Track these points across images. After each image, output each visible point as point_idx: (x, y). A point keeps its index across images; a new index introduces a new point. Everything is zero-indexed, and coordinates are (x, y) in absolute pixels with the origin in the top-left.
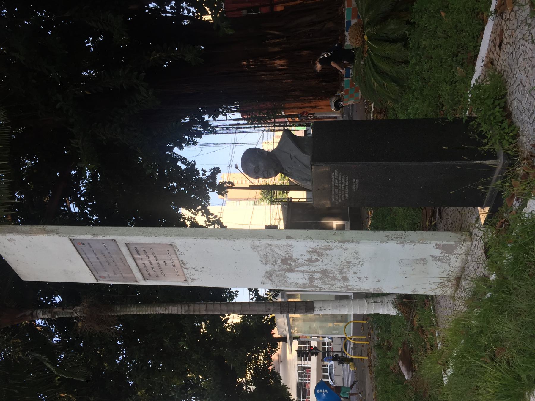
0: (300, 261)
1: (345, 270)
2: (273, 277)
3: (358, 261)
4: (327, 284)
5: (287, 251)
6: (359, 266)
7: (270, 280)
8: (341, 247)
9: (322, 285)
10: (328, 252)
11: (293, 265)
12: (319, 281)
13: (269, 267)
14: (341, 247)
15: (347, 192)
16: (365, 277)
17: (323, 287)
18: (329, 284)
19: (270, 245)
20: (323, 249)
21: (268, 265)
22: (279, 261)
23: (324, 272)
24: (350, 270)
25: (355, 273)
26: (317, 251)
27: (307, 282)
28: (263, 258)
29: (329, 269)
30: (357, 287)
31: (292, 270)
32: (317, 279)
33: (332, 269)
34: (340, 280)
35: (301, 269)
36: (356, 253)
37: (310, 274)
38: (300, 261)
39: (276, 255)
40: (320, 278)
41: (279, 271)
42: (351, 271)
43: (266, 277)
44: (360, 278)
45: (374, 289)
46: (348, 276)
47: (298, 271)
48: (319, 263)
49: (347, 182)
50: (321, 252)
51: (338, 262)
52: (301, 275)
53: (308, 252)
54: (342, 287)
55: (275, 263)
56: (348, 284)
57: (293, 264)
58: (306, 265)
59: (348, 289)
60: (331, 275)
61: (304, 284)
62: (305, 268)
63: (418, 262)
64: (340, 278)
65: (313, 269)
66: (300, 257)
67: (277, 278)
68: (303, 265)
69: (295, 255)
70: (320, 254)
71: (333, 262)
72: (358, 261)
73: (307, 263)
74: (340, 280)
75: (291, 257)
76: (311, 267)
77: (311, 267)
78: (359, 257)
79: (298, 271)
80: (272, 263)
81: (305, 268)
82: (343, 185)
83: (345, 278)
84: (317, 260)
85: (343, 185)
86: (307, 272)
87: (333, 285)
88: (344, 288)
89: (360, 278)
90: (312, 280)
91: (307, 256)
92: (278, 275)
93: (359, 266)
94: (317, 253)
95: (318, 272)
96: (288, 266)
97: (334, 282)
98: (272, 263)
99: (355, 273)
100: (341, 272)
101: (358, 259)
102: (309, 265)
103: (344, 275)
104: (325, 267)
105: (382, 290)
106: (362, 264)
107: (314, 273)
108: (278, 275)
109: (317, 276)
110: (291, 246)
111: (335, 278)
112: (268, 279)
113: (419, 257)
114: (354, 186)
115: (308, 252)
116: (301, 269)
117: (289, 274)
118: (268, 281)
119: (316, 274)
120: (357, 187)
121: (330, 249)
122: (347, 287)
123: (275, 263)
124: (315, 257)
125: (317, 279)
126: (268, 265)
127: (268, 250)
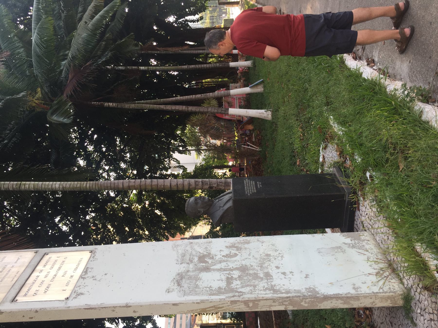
0: (218, 257)
1: (266, 265)
2: (184, 280)
3: (277, 253)
4: (247, 286)
5: (206, 248)
6: (280, 258)
7: (179, 285)
8: (258, 240)
9: (242, 287)
10: (246, 246)
11: (210, 262)
12: (238, 282)
13: (182, 268)
14: (258, 240)
15: (255, 188)
16: (291, 272)
17: (243, 290)
18: (251, 286)
19: (192, 243)
20: (242, 243)
21: (183, 264)
22: (196, 259)
23: (243, 269)
24: (272, 264)
25: (277, 267)
26: (236, 245)
27: (223, 284)
28: (180, 257)
29: (248, 264)
30: (285, 287)
31: (207, 269)
32: (236, 279)
33: (252, 264)
34: (262, 279)
35: (218, 266)
36: (273, 245)
37: (228, 272)
38: (218, 257)
39: (194, 253)
40: (239, 277)
41: (193, 271)
42: (273, 265)
43: (175, 280)
44: (284, 273)
45: (306, 289)
46: (270, 271)
47: (214, 270)
49: (254, 184)
50: (240, 246)
51: (257, 256)
52: (216, 275)
53: (227, 247)
54: (266, 289)
55: (191, 261)
56: (273, 283)
57: (210, 261)
58: (224, 261)
59: (275, 291)
60: (251, 272)
61: (220, 288)
62: (223, 265)
63: (336, 251)
64: (262, 275)
65: (231, 265)
66: (218, 253)
67: (188, 281)
68: (220, 262)
69: (213, 252)
70: (238, 249)
71: (252, 256)
72: (277, 253)
73: (226, 259)
74: (262, 279)
75: (210, 254)
76: (229, 264)
77: (229, 264)
78: (277, 249)
79: (214, 270)
80: (188, 261)
81: (223, 265)
82: (252, 185)
83: (268, 275)
84: (236, 255)
85: (252, 185)
86: (225, 270)
87: (255, 286)
88: (270, 290)
89: (284, 273)
90: (229, 280)
91: (226, 252)
93: (280, 258)
94: (235, 247)
95: (237, 269)
96: (204, 264)
97: (257, 282)
98: (188, 261)
99: (277, 267)
100: (261, 267)
101: (276, 251)
102: (227, 261)
103: (266, 271)
104: (244, 263)
105: (317, 290)
106: (282, 257)
107: (232, 270)
108: (190, 278)
109: (236, 274)
110: (211, 242)
111: (256, 276)
112: (176, 284)
113: (334, 246)
114: (258, 186)
115: (227, 247)
116: (218, 266)
117: (204, 275)
118: (176, 286)
119: (234, 272)
120: (261, 186)
121: (248, 243)
122: (273, 289)
123: (191, 261)
124: (234, 251)
125: (236, 279)
126: (184, 265)
127: (188, 248)
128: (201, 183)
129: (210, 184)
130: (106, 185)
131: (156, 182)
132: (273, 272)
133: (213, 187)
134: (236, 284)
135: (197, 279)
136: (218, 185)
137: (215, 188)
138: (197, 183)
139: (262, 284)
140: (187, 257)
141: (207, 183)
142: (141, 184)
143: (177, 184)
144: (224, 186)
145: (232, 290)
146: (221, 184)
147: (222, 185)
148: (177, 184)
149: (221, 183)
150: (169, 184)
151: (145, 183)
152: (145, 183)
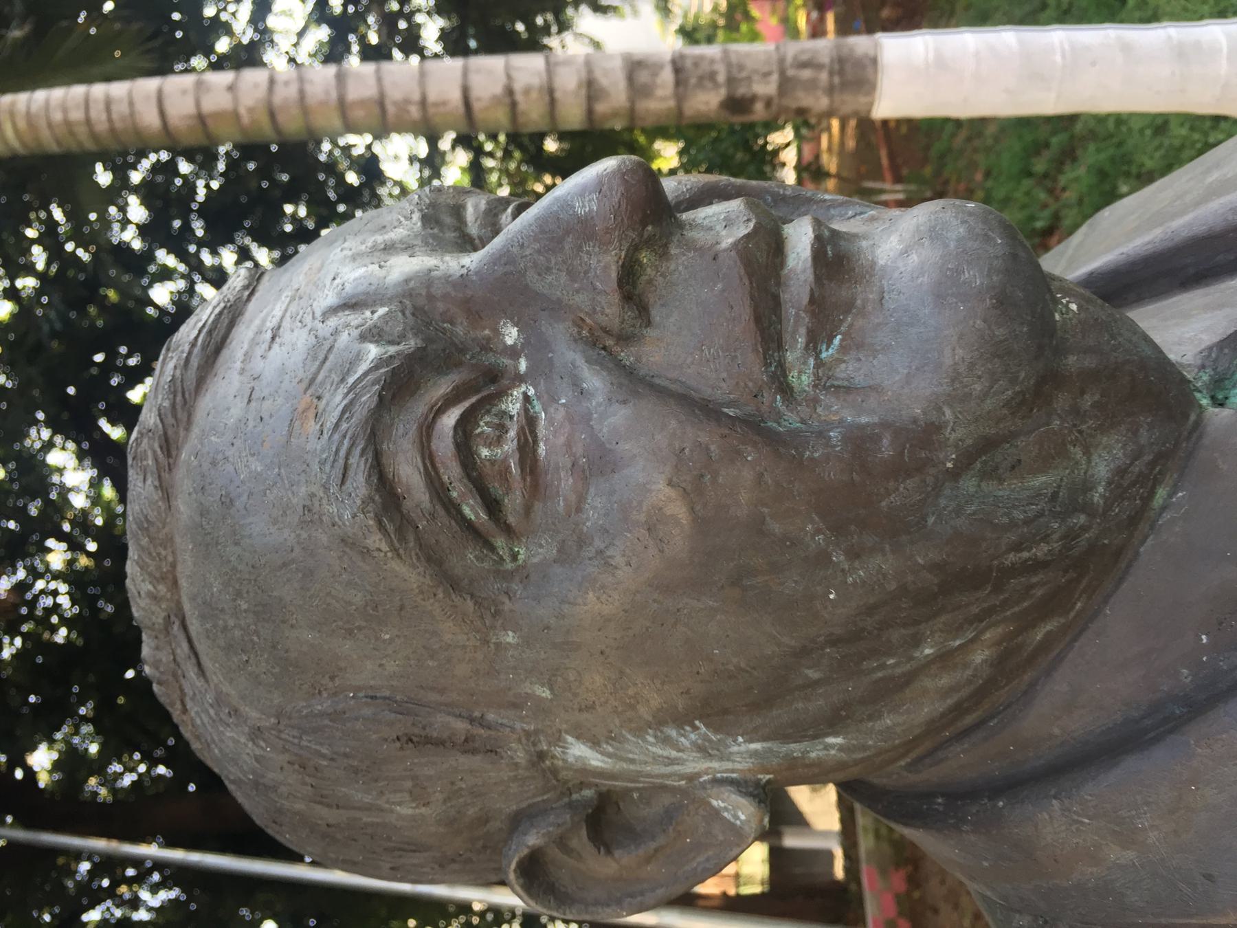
128: (667, 76)
129: (731, 81)
130: (58, 116)
131: (372, 81)
133: (753, 99)
136: (786, 84)
137: (768, 103)
138: (643, 77)
141: (712, 76)
142: (278, 99)
143: (510, 92)
144: (830, 90)
146: (806, 74)
147: (812, 85)
148: (510, 92)
149: (804, 65)
150: (455, 96)
151: (302, 93)
152: (302, 93)
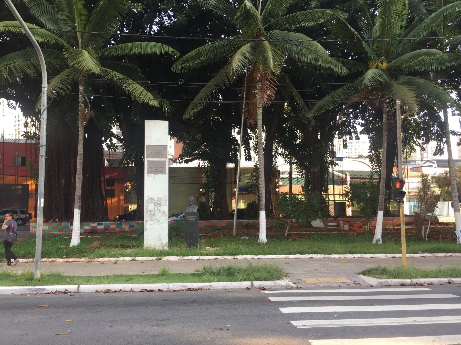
13: (156, 199)
27: (149, 209)
31: (155, 205)
38: (159, 208)
48: (159, 213)
68: (158, 209)
70: (163, 214)
83: (152, 220)
90: (151, 211)
91: (161, 210)
92: (152, 201)
108: (152, 201)
109: (153, 213)
111: (151, 217)
117: (153, 205)
121: (165, 216)
122: (147, 221)
132: (153, 222)
134: (149, 213)
135: (151, 203)
139: (148, 219)
140: (160, 200)
145: (147, 211)
